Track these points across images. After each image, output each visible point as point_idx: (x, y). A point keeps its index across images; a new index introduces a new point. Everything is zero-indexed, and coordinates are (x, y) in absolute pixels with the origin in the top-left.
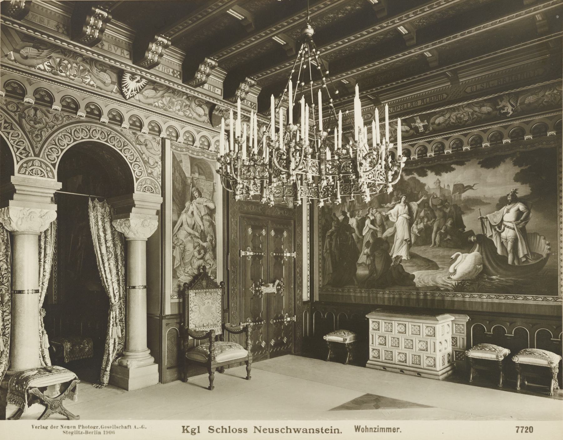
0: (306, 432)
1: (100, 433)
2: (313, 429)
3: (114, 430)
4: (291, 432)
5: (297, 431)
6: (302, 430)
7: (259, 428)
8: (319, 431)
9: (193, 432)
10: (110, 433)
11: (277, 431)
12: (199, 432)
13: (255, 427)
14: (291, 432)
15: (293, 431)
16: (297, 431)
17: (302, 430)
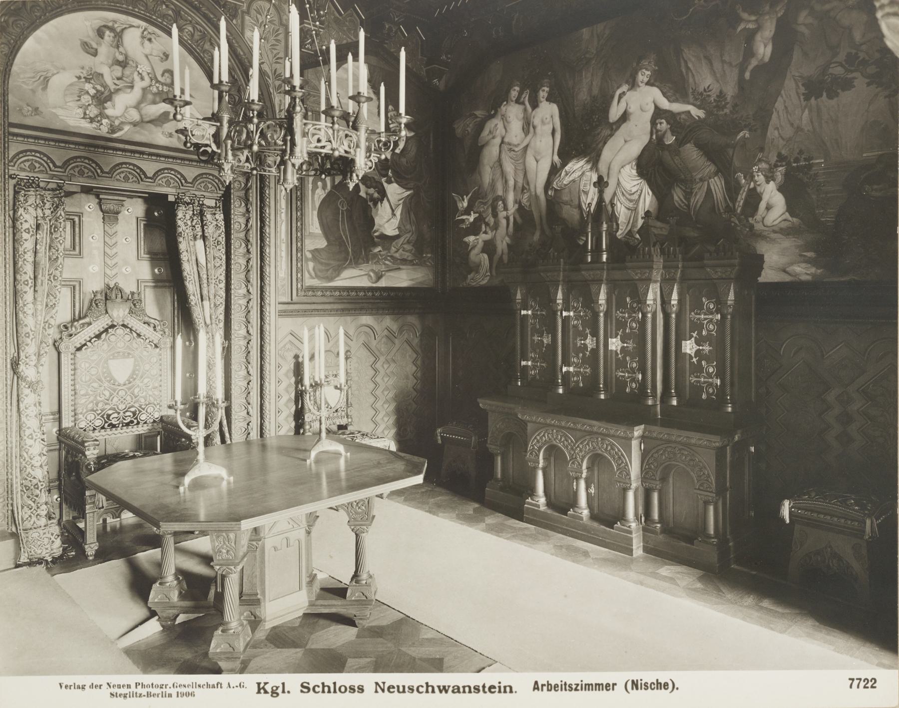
0: (459, 692)
1: (170, 695)
2: (470, 687)
3: (194, 690)
5: (444, 689)
6: (451, 689)
7: (382, 685)
8: (479, 691)
9: (274, 693)
10: (188, 694)
11: (411, 689)
13: (377, 684)
14: (433, 691)
15: (436, 689)
16: (444, 689)
17: (451, 689)
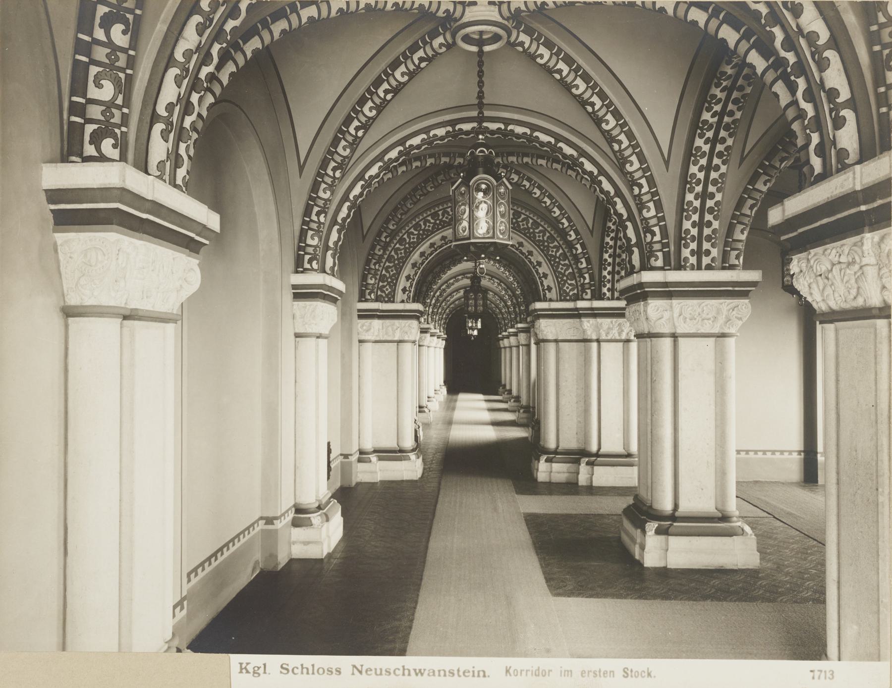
2: (445, 671)
4: (409, 675)
6: (426, 672)
7: (360, 668)
8: (453, 674)
11: (388, 672)
12: (265, 673)
13: (354, 666)
14: (409, 675)
15: (413, 673)
16: (419, 672)
